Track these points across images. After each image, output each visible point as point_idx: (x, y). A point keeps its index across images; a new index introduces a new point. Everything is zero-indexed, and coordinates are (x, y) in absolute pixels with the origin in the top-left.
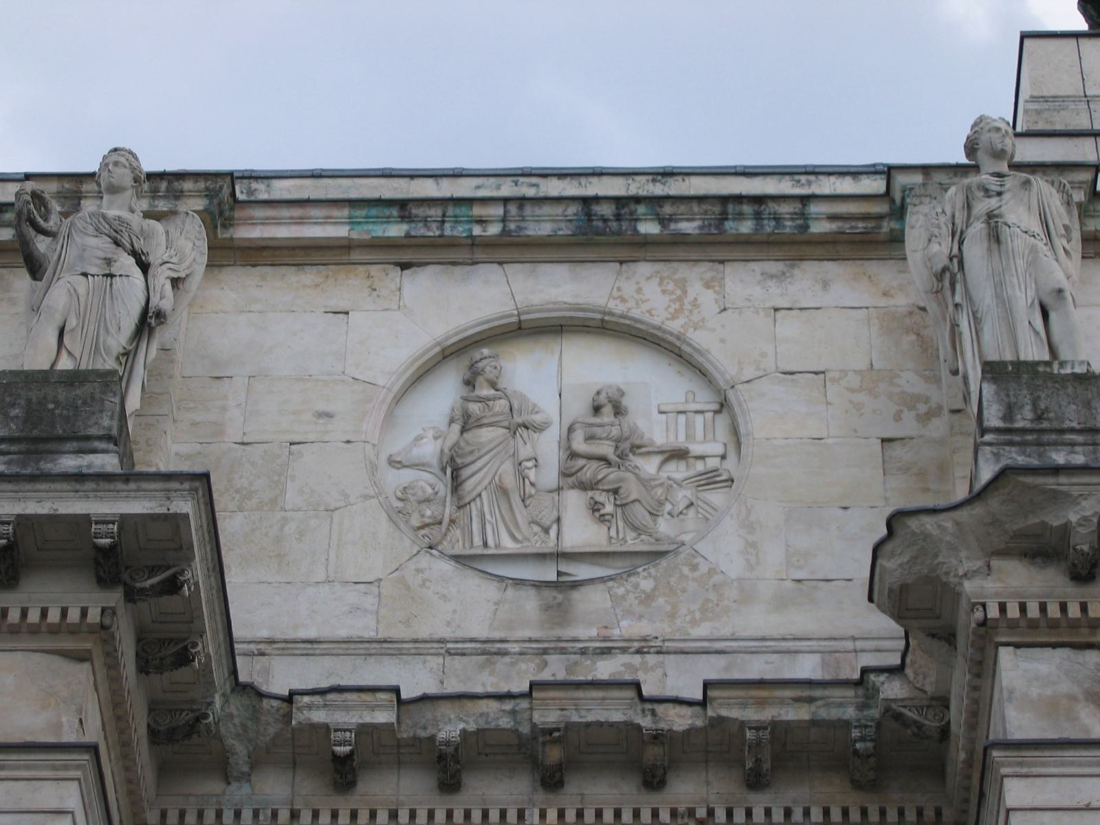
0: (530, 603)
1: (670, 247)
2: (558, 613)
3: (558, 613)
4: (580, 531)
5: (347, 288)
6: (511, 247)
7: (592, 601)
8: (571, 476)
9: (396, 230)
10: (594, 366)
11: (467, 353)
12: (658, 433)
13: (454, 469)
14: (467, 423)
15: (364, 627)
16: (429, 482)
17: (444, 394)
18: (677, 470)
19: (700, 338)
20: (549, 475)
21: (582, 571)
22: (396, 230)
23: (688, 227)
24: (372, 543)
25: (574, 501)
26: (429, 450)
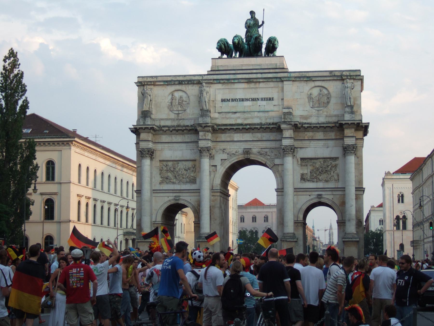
0: (176, 115)
1: (185, 84)
2: (178, 116)
3: (178, 116)
4: (180, 109)
5: (163, 88)
6: (174, 84)
7: (180, 115)
8: (179, 104)
9: (166, 83)
10: (180, 93)
11: (172, 94)
13: (171, 103)
14: (172, 100)
15: (166, 117)
16: (170, 104)
17: (170, 97)
18: (186, 103)
19: (187, 92)
20: (177, 103)
21: (180, 112)
22: (166, 83)
23: (186, 83)
24: (166, 111)
25: (179, 106)
26: (170, 101)
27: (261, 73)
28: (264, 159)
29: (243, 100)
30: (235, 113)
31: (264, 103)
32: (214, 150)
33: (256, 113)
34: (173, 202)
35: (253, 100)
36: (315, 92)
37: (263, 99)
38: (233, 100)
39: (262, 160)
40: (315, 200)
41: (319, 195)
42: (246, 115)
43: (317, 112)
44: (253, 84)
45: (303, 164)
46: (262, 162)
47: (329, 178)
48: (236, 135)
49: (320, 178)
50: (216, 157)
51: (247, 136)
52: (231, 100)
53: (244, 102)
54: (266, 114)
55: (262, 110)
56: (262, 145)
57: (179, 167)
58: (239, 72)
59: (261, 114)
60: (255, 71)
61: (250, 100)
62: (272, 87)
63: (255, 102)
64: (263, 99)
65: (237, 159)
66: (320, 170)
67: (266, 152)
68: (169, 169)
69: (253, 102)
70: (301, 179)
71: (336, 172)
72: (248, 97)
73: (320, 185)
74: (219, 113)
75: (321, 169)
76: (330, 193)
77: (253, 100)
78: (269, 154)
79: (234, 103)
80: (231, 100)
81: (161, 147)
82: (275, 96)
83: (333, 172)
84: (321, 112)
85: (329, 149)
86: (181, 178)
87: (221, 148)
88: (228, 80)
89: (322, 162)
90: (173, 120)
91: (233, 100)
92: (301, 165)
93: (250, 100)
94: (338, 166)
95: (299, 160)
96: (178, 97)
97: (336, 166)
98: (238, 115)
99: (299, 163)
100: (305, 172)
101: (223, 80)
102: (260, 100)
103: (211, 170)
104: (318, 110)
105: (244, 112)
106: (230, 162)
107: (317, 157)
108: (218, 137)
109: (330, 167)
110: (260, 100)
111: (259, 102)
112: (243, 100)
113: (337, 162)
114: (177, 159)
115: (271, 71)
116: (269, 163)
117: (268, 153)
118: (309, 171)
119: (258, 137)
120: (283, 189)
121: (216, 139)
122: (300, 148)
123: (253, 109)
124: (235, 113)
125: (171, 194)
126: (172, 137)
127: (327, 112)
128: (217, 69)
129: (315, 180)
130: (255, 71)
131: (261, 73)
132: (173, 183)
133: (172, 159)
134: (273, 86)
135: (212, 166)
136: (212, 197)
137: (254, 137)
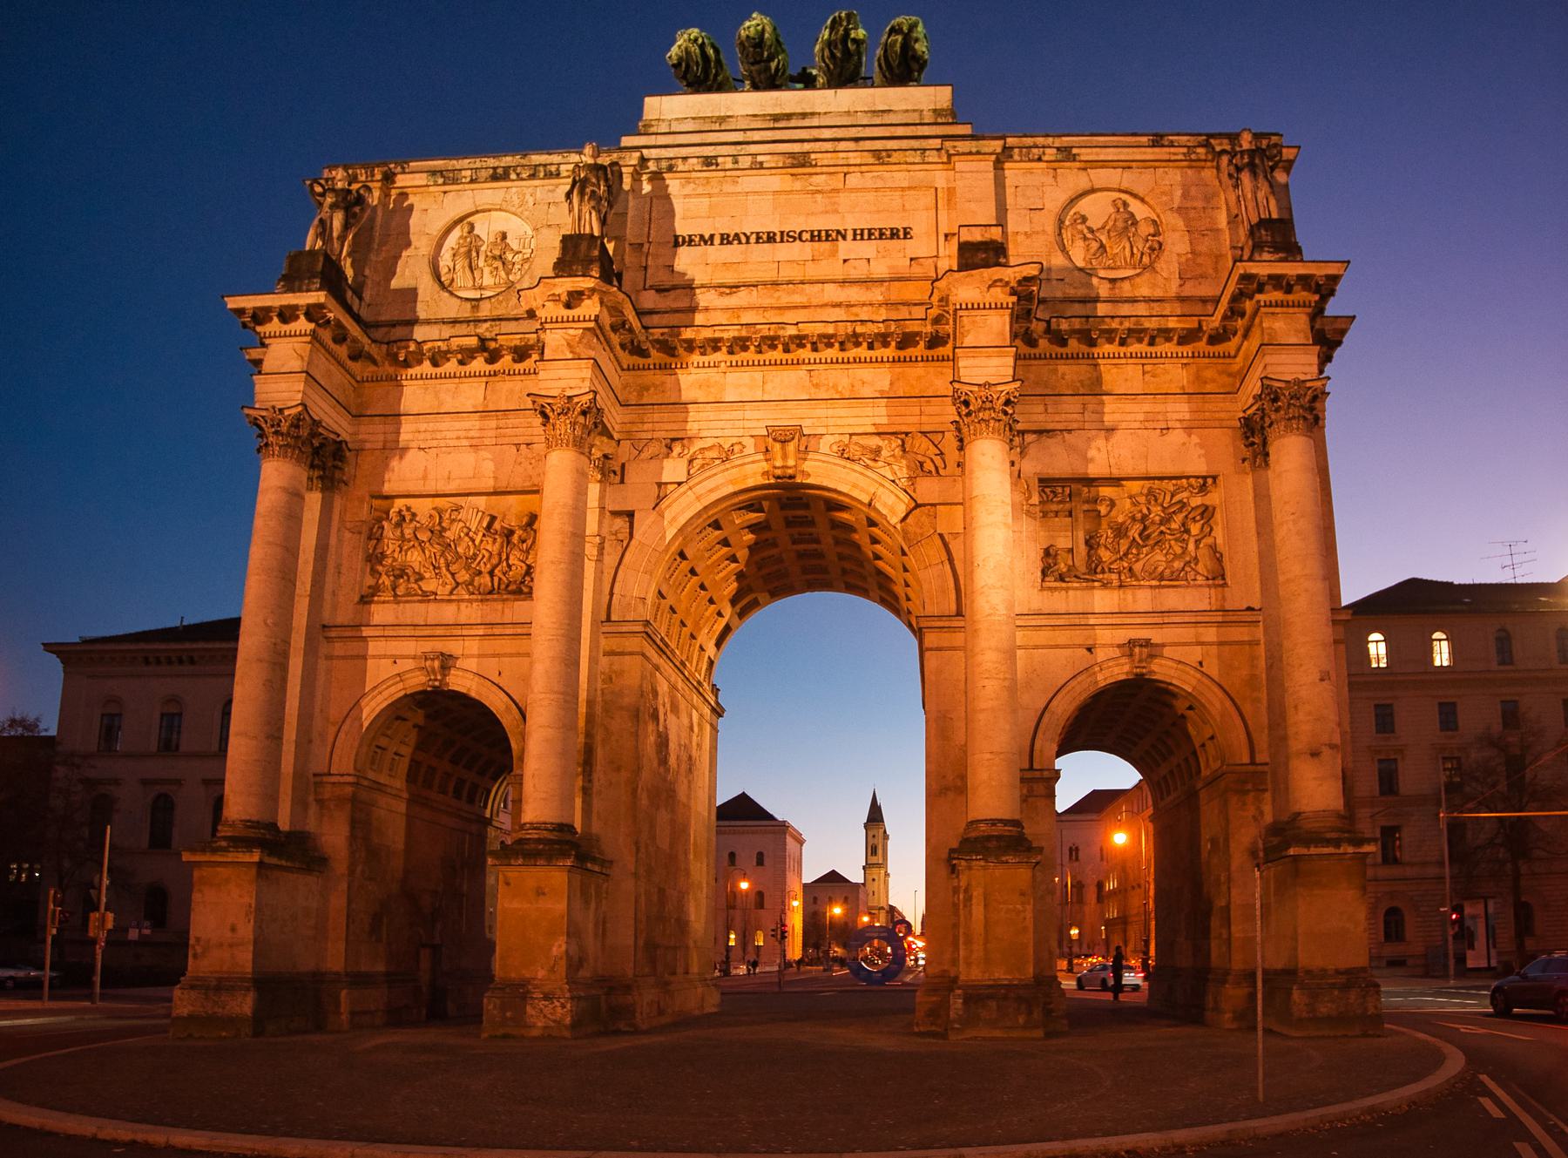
0: (468, 305)
3: (475, 308)
4: (488, 280)
12: (515, 245)
18: (518, 258)
27: (857, 140)
28: (862, 482)
29: (771, 238)
30: (735, 287)
31: (868, 248)
32: (626, 444)
33: (832, 293)
34: (417, 681)
35: (816, 237)
36: (1097, 209)
37: (858, 235)
38: (726, 239)
39: (855, 486)
40: (1116, 670)
41: (1132, 643)
42: (784, 297)
43: (1108, 285)
44: (819, 180)
45: (1054, 507)
46: (855, 494)
47: (1177, 565)
48: (734, 377)
49: (1137, 567)
50: (631, 476)
51: (786, 382)
52: (717, 240)
53: (778, 245)
54: (877, 294)
55: (855, 274)
56: (851, 421)
57: (457, 527)
58: (757, 136)
59: (854, 294)
60: (827, 134)
61: (806, 236)
62: (903, 189)
63: (826, 246)
64: (858, 235)
65: (732, 482)
66: (1134, 532)
67: (877, 451)
68: (408, 532)
69: (816, 244)
70: (1044, 573)
71: (1209, 540)
72: (795, 225)
73: (1142, 599)
74: (659, 290)
75: (1138, 527)
76: (1187, 634)
77: (816, 237)
78: (891, 460)
79: (733, 252)
80: (717, 240)
81: (381, 437)
82: (920, 223)
83: (1197, 542)
84: (1126, 286)
85: (1177, 436)
86: (463, 576)
87: (663, 434)
88: (709, 161)
89: (1142, 499)
90: (455, 322)
91: (726, 239)
92: (1045, 515)
93: (806, 236)
94: (1218, 515)
95: (1035, 484)
96: (484, 237)
97: (1207, 513)
98: (742, 298)
99: (1035, 499)
100: (1063, 542)
101: (685, 159)
102: (850, 236)
103: (605, 532)
104: (1113, 281)
105: (775, 284)
106: (698, 498)
107: (1116, 473)
108: (647, 389)
109: (1179, 518)
110: (850, 236)
111: (845, 248)
112: (771, 238)
113: (1213, 498)
114: (452, 487)
115: (900, 131)
116: (891, 500)
117: (885, 453)
118: (1081, 536)
119: (835, 387)
120: (959, 613)
121: (640, 395)
122: (1040, 432)
123: (813, 272)
124: (735, 287)
125: (410, 647)
126: (437, 394)
127: (1154, 286)
128: (664, 128)
129: (1114, 576)
130: (827, 134)
131: (857, 140)
132: (426, 597)
133: (431, 488)
134: (905, 184)
135: (615, 514)
136: (604, 661)
137: (817, 386)
